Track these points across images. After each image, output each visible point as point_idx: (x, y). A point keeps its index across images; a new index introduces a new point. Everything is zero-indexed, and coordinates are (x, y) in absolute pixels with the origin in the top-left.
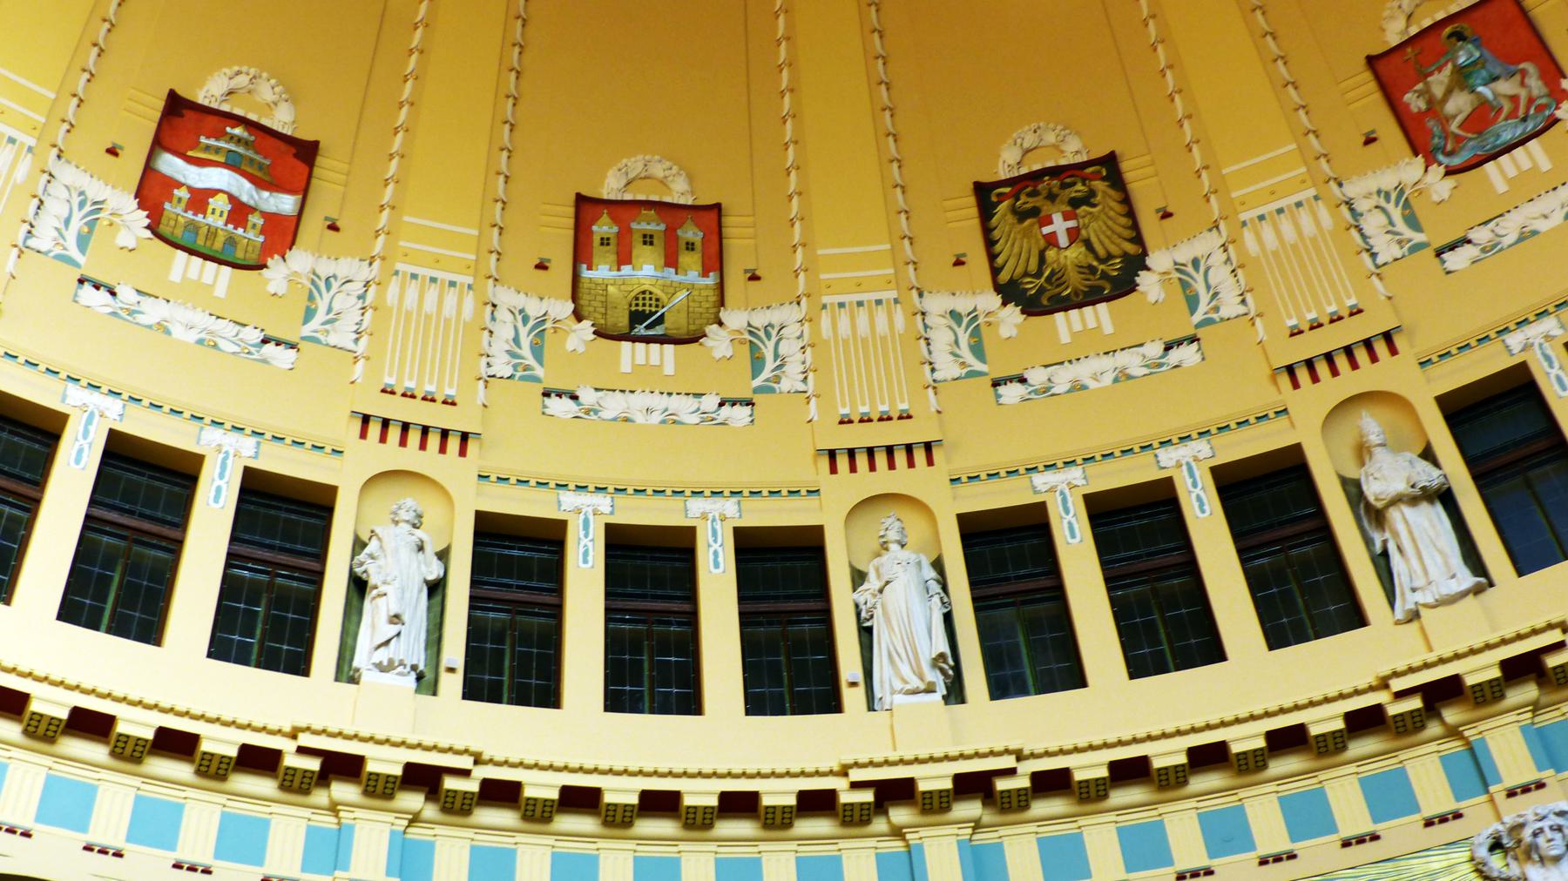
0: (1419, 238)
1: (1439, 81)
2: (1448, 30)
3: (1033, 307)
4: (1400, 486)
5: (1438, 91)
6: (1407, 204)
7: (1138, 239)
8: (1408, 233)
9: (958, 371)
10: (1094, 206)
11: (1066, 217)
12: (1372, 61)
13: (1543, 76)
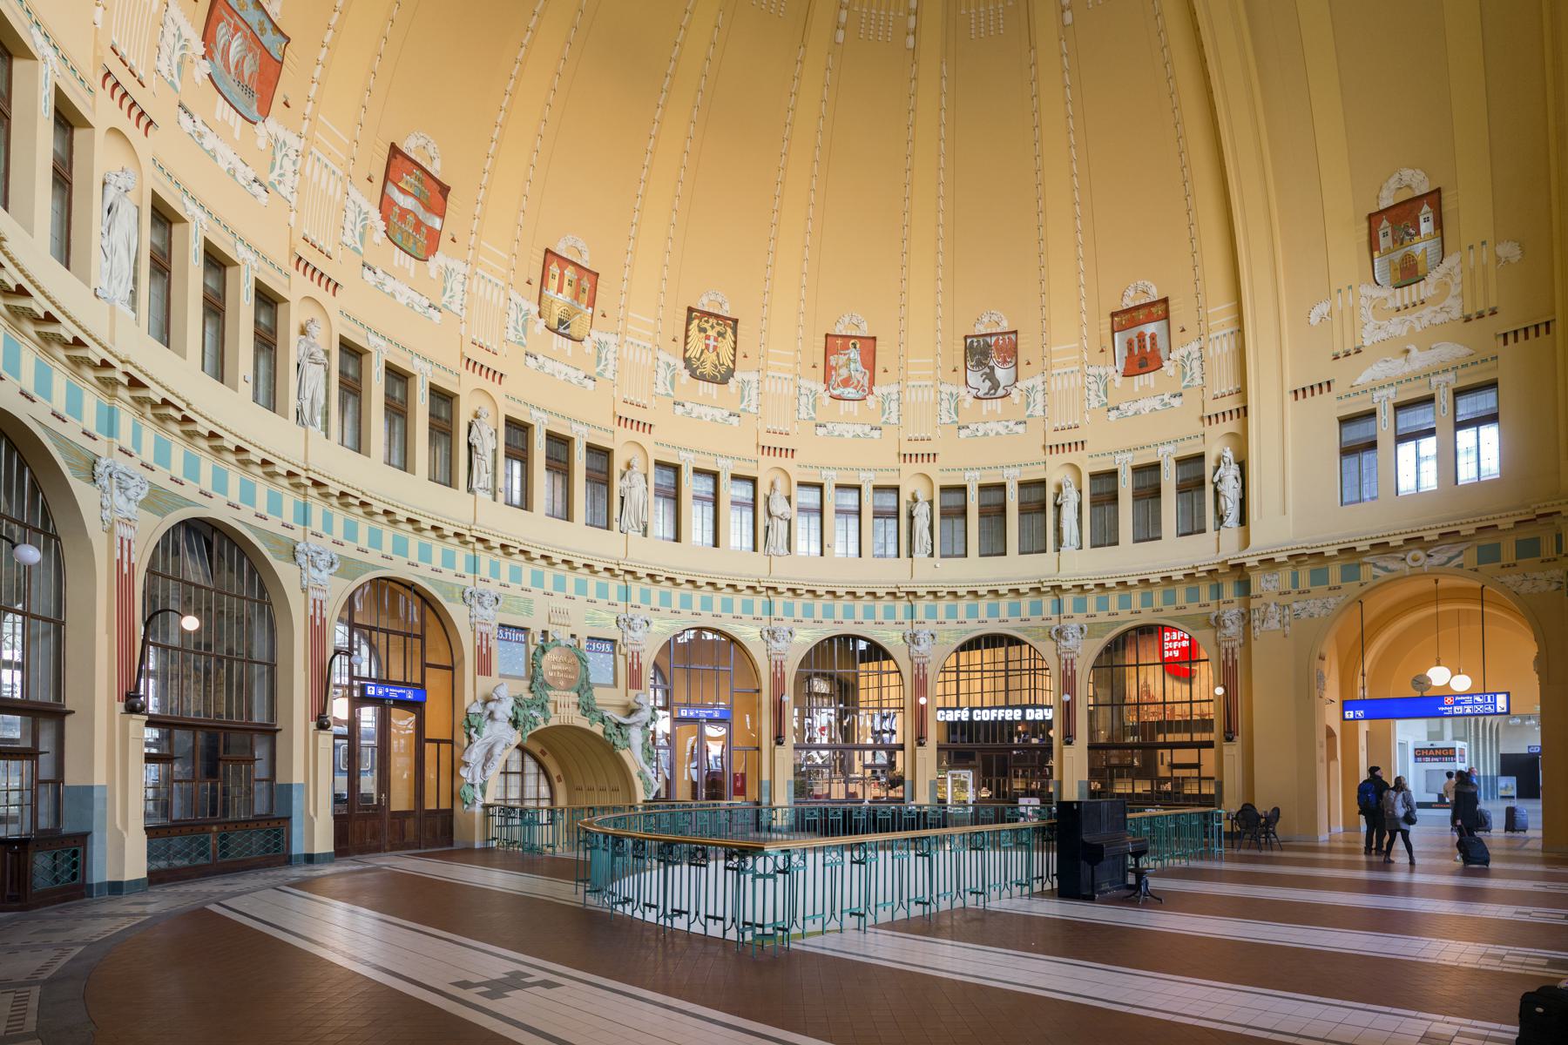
0: (813, 415)
1: (843, 359)
2: (853, 341)
3: (693, 375)
4: (779, 513)
5: (840, 363)
6: (815, 400)
7: (734, 362)
8: (811, 412)
9: (664, 392)
10: (724, 338)
11: (716, 340)
12: (827, 335)
13: (869, 379)
